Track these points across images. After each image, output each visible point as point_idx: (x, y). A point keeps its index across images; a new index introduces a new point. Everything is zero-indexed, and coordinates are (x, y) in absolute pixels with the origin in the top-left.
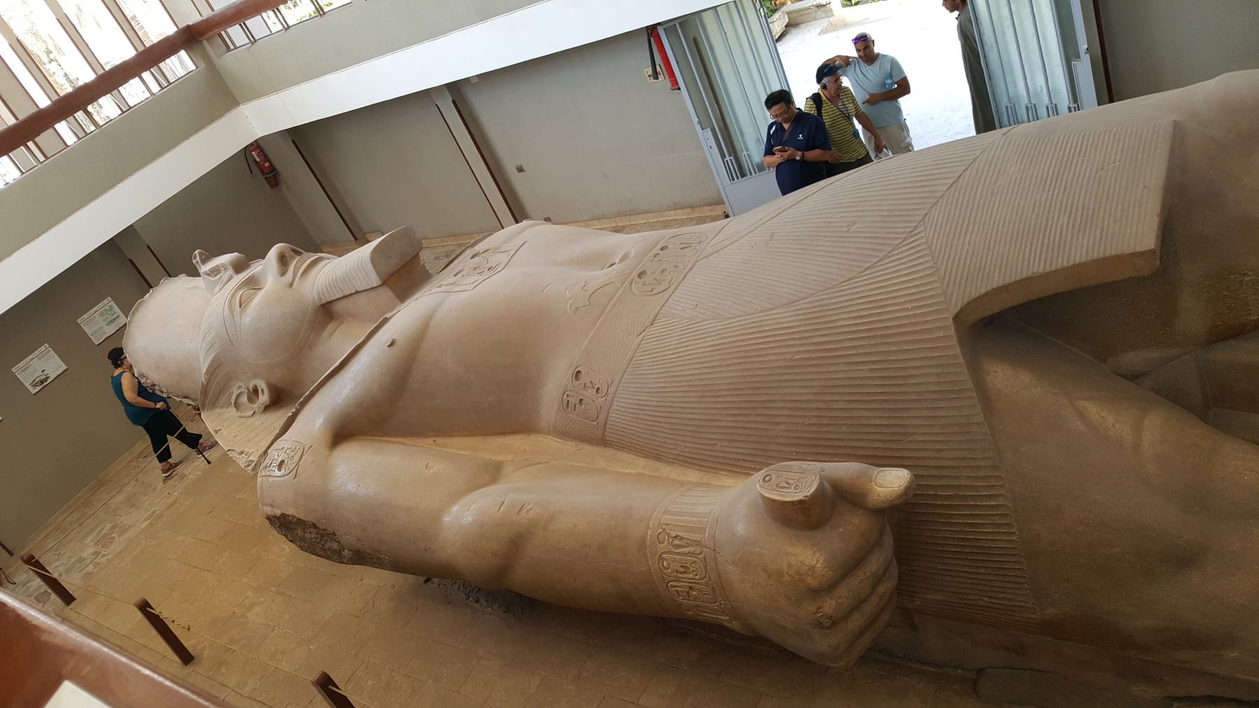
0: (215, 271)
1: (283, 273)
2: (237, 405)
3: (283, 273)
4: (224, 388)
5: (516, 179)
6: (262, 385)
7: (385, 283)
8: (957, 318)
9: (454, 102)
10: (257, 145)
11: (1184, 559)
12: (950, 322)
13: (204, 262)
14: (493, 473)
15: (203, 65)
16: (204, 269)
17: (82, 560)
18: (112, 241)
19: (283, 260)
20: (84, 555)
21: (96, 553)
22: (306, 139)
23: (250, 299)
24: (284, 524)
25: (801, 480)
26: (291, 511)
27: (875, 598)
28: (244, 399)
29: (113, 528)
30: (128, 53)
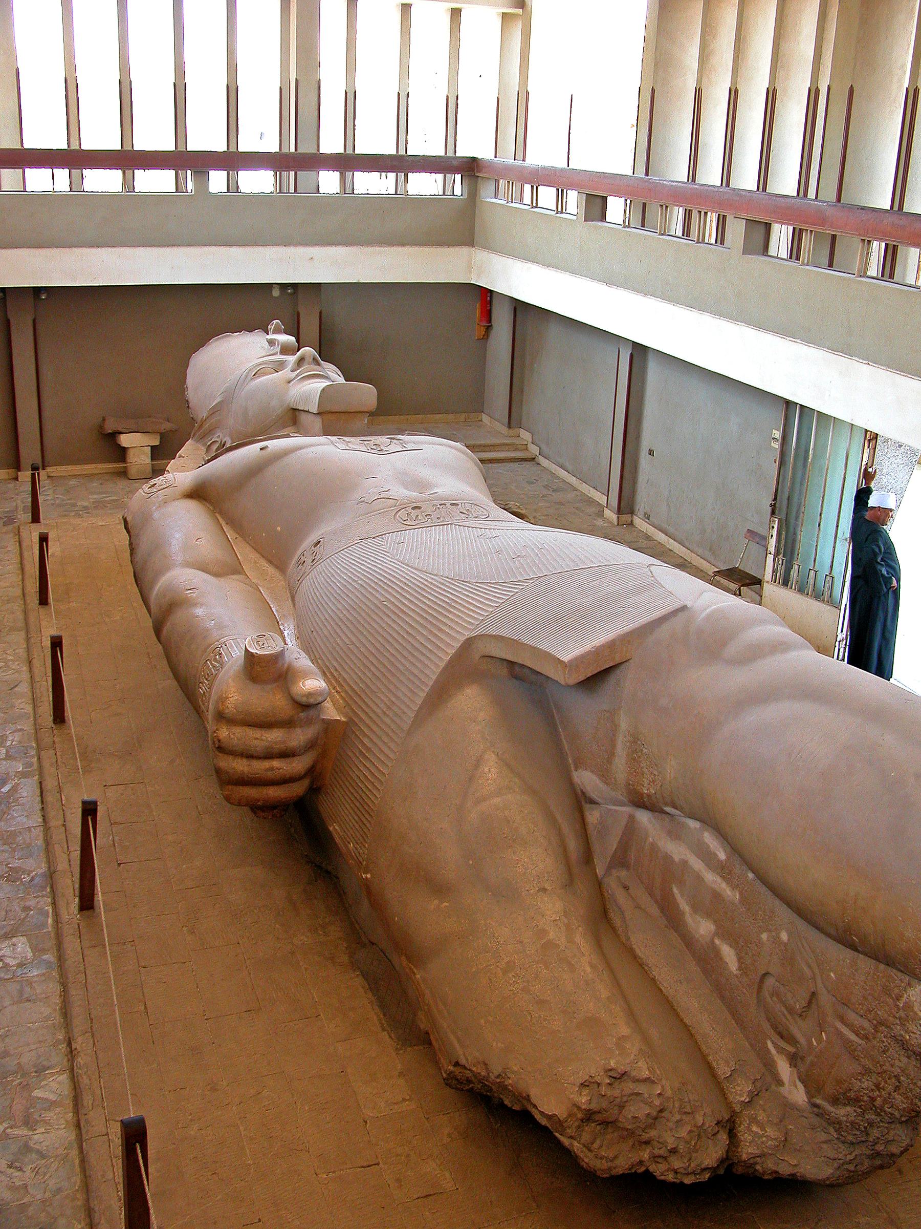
0: (271, 343)
2: (208, 448)
4: (210, 431)
5: (644, 461)
8: (469, 642)
9: (631, 356)
10: (491, 291)
11: (440, 889)
13: (274, 333)
14: (228, 569)
15: (465, 196)
16: (271, 336)
17: (74, 505)
18: (295, 286)
19: (301, 361)
21: (86, 508)
23: (265, 374)
27: (266, 764)
29: (114, 501)
30: (436, 149)
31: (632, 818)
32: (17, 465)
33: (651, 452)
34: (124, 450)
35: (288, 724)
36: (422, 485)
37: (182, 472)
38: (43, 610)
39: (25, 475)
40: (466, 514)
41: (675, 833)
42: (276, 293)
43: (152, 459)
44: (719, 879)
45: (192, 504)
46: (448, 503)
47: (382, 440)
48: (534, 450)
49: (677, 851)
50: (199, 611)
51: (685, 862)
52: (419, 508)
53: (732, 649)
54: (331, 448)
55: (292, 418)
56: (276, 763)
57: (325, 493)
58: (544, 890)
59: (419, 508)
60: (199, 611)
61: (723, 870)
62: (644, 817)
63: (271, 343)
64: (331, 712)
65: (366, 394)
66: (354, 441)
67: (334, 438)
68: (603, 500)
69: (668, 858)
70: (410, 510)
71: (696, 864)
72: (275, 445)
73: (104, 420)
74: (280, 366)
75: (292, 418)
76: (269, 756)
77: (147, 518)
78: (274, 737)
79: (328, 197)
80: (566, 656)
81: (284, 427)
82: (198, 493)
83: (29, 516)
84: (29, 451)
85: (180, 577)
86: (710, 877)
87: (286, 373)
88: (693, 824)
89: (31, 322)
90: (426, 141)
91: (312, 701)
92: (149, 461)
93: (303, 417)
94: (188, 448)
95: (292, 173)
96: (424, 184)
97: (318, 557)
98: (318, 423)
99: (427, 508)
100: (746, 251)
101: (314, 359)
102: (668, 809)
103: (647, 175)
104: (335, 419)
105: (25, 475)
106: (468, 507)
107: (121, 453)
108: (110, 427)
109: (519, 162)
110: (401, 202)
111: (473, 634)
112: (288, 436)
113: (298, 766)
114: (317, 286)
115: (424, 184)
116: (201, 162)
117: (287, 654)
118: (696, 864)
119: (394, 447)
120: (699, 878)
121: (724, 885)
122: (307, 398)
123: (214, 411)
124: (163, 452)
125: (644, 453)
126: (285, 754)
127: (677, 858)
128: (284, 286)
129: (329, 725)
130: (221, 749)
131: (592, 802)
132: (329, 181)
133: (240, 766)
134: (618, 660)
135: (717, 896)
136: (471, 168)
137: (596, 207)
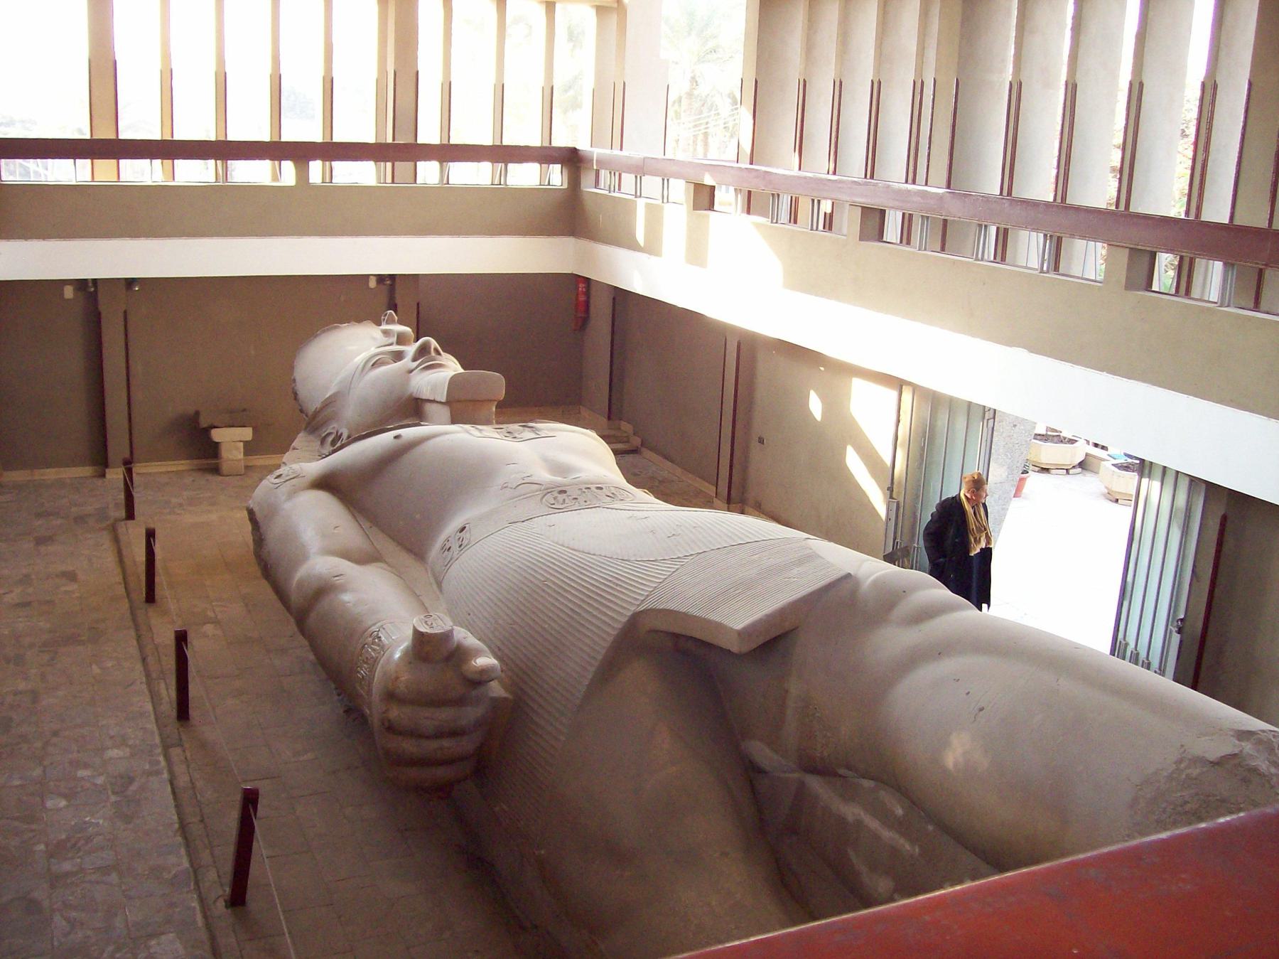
0: (386, 333)
1: (414, 360)
2: (323, 441)
3: (414, 360)
4: (326, 422)
6: (345, 436)
7: (448, 403)
10: (587, 281)
12: (629, 614)
13: (388, 323)
15: (565, 186)
16: (384, 327)
18: (392, 277)
19: (423, 351)
20: (174, 500)
21: (181, 505)
22: (621, 297)
24: (251, 513)
25: (440, 624)
26: (256, 509)
27: (434, 744)
28: (330, 439)
30: (534, 139)
31: (802, 784)
32: (101, 461)
33: (761, 441)
34: (217, 444)
35: (460, 702)
36: (561, 469)
37: (305, 462)
38: (151, 611)
39: (116, 475)
40: (612, 496)
41: (849, 794)
42: (373, 283)
43: (246, 454)
44: (897, 836)
45: (323, 497)
46: (593, 487)
47: (515, 427)
48: (636, 441)
49: (852, 812)
50: (346, 597)
51: (859, 824)
52: (565, 492)
53: (902, 609)
54: (466, 436)
55: (414, 409)
56: (446, 743)
57: (467, 478)
58: (725, 854)
59: (565, 492)
60: (346, 597)
61: (901, 826)
62: (815, 784)
63: (386, 333)
64: (496, 689)
65: (495, 383)
66: (488, 430)
67: (467, 427)
68: (711, 490)
69: (842, 820)
70: (556, 494)
71: (873, 824)
72: (409, 433)
73: (197, 413)
74: (398, 356)
75: (414, 409)
76: (439, 734)
77: (273, 510)
78: (445, 715)
79: (427, 189)
80: (739, 626)
81: (407, 417)
82: (326, 483)
83: (123, 513)
84: (118, 447)
85: (319, 564)
86: (886, 834)
87: (407, 362)
88: (867, 784)
89: (121, 315)
90: (523, 131)
91: (485, 677)
92: (241, 456)
93: (429, 408)
94: (301, 440)
95: (389, 165)
96: (525, 176)
97: (465, 542)
98: (445, 412)
99: (573, 492)
100: (863, 237)
101: (436, 350)
102: (842, 771)
103: (751, 163)
104: (462, 407)
105: (116, 475)
106: (613, 490)
107: (213, 450)
108: (204, 423)
109: (616, 152)
110: (499, 193)
111: (641, 608)
112: (418, 425)
113: (466, 745)
114: (415, 277)
115: (525, 176)
116: (301, 153)
117: (455, 633)
118: (873, 824)
119: (528, 434)
120: (877, 837)
121: (902, 841)
122: (434, 388)
123: (329, 403)
124: (269, 444)
125: (754, 443)
126: (454, 733)
127: (850, 818)
128: (381, 278)
129: (496, 703)
130: (391, 728)
131: (760, 771)
132: (428, 172)
133: (409, 747)
134: (787, 626)
135: (894, 852)
136: (572, 159)
137: (704, 198)
